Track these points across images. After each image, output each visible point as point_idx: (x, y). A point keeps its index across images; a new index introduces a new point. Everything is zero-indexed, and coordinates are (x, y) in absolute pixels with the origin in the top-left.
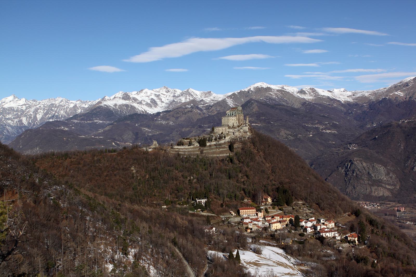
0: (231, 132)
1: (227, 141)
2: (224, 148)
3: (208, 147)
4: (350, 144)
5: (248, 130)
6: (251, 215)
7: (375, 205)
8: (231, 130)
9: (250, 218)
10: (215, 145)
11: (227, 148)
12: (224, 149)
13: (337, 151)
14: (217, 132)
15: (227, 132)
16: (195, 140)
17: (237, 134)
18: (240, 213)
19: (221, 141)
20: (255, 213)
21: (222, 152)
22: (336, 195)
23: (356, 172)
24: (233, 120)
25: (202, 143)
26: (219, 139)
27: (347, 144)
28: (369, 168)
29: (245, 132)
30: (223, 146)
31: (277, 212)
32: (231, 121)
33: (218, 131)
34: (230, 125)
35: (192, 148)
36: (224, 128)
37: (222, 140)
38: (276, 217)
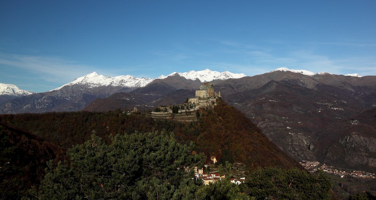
2: (193, 115)
3: (178, 114)
4: (353, 120)
5: (215, 101)
7: (371, 175)
11: (194, 115)
13: (340, 126)
14: (190, 102)
15: (198, 103)
19: (191, 110)
21: (189, 119)
23: (354, 144)
25: (175, 110)
27: (350, 120)
28: (366, 141)
29: (213, 103)
34: (201, 97)
35: (165, 114)
36: (195, 99)
37: (193, 109)
38: (213, 175)
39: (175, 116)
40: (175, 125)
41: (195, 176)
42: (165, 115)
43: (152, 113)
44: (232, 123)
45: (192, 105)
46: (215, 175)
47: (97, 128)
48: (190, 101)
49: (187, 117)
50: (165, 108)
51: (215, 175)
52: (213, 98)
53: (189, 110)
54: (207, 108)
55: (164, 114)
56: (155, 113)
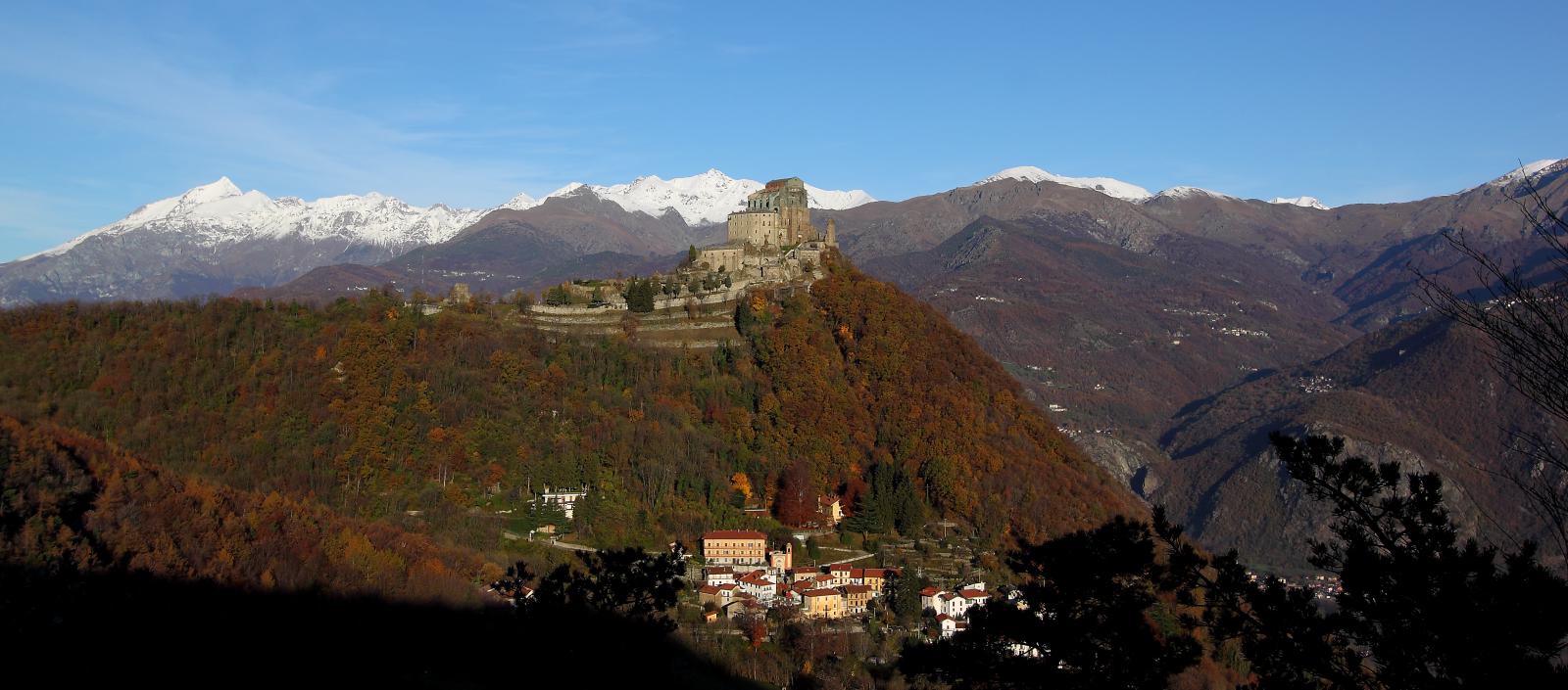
0: (755, 267)
1: (731, 296)
2: (721, 319)
5: (817, 262)
6: (747, 560)
8: (756, 261)
9: (732, 572)
10: (686, 308)
11: (727, 320)
12: (718, 325)
14: (706, 266)
15: (741, 267)
16: (613, 288)
17: (774, 271)
18: (706, 552)
20: (763, 553)
21: (704, 335)
22: (1100, 504)
24: (767, 224)
26: (705, 289)
30: (715, 314)
31: (855, 555)
32: (757, 227)
33: (709, 261)
35: (597, 316)
36: (729, 252)
38: (838, 573)
39: (639, 323)
40: (647, 359)
41: (762, 578)
42: (598, 322)
43: (535, 309)
44: (901, 350)
45: (714, 279)
46: (848, 573)
47: (288, 374)
48: (704, 260)
49: (697, 327)
50: (592, 289)
51: (848, 573)
52: (808, 246)
53: (701, 297)
54: (784, 291)
55: (591, 315)
56: (552, 310)
